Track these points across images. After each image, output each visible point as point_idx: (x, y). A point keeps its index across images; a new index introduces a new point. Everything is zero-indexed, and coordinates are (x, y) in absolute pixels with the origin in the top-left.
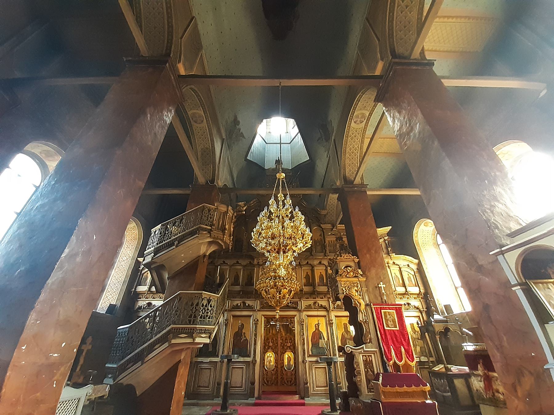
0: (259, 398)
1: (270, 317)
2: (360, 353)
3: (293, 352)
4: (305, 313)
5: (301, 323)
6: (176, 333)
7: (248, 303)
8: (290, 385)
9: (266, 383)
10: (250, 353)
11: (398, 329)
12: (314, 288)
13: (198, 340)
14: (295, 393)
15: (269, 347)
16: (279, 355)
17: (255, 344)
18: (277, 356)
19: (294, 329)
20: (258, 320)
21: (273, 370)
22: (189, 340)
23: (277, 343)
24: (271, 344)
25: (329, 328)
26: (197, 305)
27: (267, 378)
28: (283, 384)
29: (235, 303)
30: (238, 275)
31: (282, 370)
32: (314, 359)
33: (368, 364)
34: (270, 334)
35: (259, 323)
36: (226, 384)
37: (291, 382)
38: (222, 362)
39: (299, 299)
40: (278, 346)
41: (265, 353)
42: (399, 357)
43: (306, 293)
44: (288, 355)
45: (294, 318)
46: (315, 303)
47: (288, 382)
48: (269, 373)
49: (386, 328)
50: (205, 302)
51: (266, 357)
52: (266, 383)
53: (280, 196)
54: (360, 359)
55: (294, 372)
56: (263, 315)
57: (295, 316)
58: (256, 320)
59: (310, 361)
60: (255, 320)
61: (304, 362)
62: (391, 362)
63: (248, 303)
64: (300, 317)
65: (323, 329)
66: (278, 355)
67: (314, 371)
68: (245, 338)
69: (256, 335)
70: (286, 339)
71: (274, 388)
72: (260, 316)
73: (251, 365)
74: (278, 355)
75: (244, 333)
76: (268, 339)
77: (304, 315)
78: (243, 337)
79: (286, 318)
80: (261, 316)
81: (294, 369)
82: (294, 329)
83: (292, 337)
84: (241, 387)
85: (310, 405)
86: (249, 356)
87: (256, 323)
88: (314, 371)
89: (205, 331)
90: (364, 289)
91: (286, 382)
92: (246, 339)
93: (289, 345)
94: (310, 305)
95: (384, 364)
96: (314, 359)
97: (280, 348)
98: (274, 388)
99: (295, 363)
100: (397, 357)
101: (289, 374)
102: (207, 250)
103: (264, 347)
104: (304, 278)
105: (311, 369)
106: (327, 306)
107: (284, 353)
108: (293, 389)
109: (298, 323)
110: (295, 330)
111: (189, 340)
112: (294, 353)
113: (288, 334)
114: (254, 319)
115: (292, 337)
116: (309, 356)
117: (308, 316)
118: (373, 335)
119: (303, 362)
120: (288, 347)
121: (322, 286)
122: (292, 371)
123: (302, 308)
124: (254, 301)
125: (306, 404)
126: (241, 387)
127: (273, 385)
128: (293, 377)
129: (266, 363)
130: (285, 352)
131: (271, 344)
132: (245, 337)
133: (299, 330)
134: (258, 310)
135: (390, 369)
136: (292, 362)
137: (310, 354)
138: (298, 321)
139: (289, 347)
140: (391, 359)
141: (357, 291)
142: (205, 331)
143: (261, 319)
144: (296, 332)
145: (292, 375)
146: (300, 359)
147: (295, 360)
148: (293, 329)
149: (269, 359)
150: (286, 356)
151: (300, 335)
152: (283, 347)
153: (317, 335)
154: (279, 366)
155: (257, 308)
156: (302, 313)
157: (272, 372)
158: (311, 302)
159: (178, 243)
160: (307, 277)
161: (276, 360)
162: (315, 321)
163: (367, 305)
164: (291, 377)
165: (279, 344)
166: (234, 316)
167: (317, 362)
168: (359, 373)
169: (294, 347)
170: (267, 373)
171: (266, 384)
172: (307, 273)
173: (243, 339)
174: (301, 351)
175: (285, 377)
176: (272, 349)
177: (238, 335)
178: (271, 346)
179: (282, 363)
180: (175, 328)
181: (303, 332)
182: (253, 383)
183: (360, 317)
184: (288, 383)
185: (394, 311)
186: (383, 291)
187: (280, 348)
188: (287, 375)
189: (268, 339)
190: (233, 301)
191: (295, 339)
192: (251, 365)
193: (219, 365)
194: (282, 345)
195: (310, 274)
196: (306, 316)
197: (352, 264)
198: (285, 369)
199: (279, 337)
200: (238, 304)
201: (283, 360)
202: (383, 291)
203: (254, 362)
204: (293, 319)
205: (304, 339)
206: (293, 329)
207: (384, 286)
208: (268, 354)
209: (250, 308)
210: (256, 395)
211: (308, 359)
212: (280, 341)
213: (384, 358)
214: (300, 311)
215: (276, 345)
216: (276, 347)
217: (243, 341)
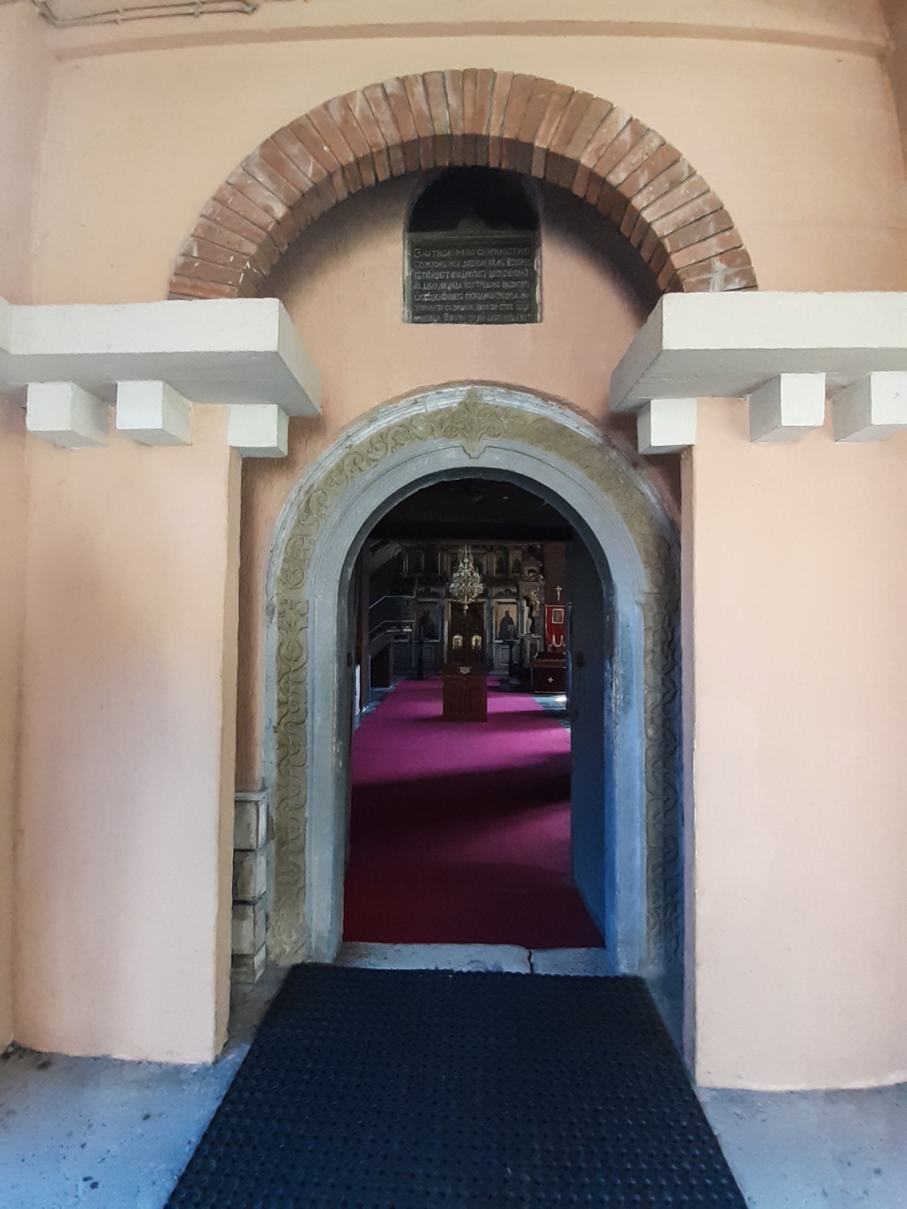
2: (529, 639)
4: (495, 600)
5: (490, 610)
6: (389, 626)
7: (432, 589)
10: (438, 634)
11: (562, 623)
13: (405, 630)
22: (399, 631)
26: (400, 606)
32: (501, 641)
33: (533, 646)
35: (446, 608)
36: (421, 660)
38: (410, 642)
42: (558, 642)
43: (497, 580)
46: (506, 591)
49: (553, 622)
50: (405, 604)
51: (454, 640)
53: (466, 560)
54: (528, 643)
56: (451, 602)
57: (485, 602)
61: (491, 643)
62: (551, 645)
63: (432, 589)
65: (513, 616)
72: (447, 604)
86: (437, 638)
87: (442, 609)
89: (408, 624)
90: (542, 592)
93: (477, 629)
95: (546, 647)
96: (501, 641)
100: (556, 641)
102: (395, 553)
104: (496, 563)
111: (399, 631)
116: (497, 639)
117: (499, 603)
118: (541, 627)
130: (474, 635)
135: (549, 650)
137: (498, 637)
138: (487, 608)
140: (551, 644)
141: (535, 593)
142: (408, 624)
144: (485, 618)
146: (488, 641)
147: (482, 640)
150: (474, 639)
153: (507, 620)
158: (502, 590)
159: (373, 554)
160: (499, 563)
161: (463, 641)
162: (504, 608)
163: (541, 604)
168: (526, 652)
169: (482, 632)
172: (501, 558)
177: (424, 621)
180: (388, 623)
183: (534, 614)
185: (563, 610)
186: (559, 593)
191: (483, 625)
195: (503, 557)
197: (536, 568)
200: (421, 592)
201: (471, 642)
202: (559, 593)
205: (492, 624)
207: (561, 589)
209: (436, 595)
211: (494, 641)
213: (546, 641)
214: (489, 598)
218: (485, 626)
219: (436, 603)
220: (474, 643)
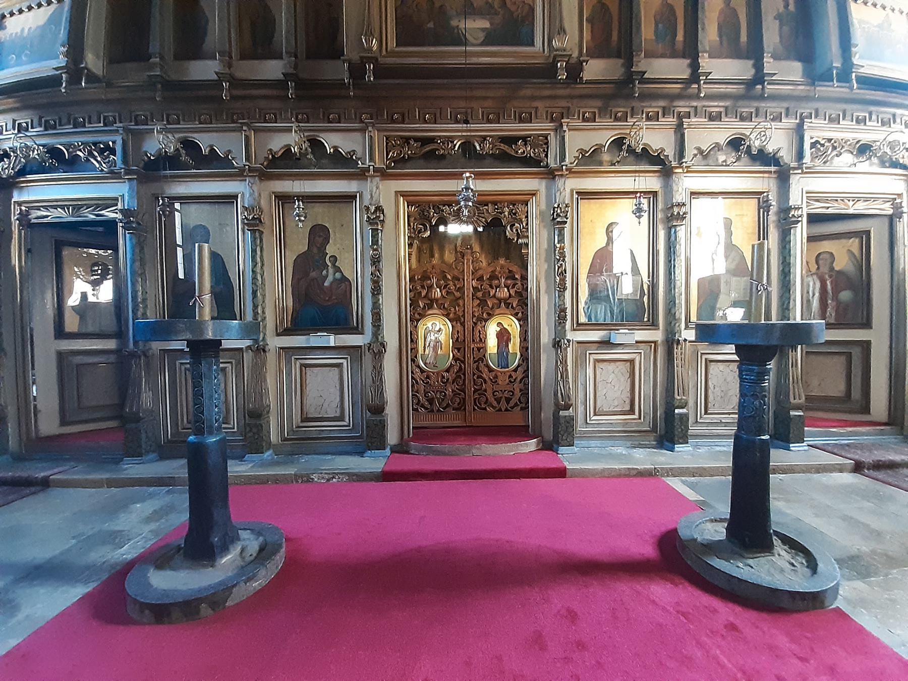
0: (401, 449)
1: (429, 203)
3: (520, 315)
4: (572, 184)
8: (506, 410)
9: (423, 406)
10: (361, 320)
12: (629, 63)
14: (520, 433)
15: (432, 301)
16: (469, 324)
17: (377, 290)
18: (459, 327)
19: (525, 240)
20: (379, 209)
21: (448, 371)
23: (461, 289)
24: (437, 293)
25: (662, 234)
27: (426, 393)
28: (483, 406)
29: (277, 143)
30: (267, 8)
31: (478, 368)
32: (595, 336)
34: (435, 261)
37: (508, 400)
39: (552, 121)
40: (462, 297)
41: (418, 321)
44: (499, 324)
45: (526, 203)
47: (498, 401)
48: (433, 377)
52: (423, 406)
55: (519, 375)
56: (404, 194)
57: (533, 194)
58: (373, 209)
59: (578, 342)
60: (368, 209)
64: (550, 197)
66: (463, 324)
67: (590, 371)
68: (338, 275)
69: (376, 261)
70: (493, 277)
71: (452, 420)
73: (368, 359)
74: (463, 324)
75: (334, 259)
76: (425, 277)
77: (568, 191)
78: (331, 270)
79: (495, 203)
80: (393, 194)
81: (519, 366)
82: (525, 240)
83: (515, 268)
84: (341, 418)
85: (583, 474)
86: (357, 330)
87: (376, 216)
88: (590, 371)
91: (492, 399)
92: (344, 279)
93: (503, 293)
94: (598, 150)
96: (595, 336)
97: (470, 305)
98: (452, 420)
99: (524, 349)
101: (503, 381)
103: (414, 303)
105: (580, 361)
106: (670, 152)
107: (486, 320)
108: (515, 418)
109: (542, 221)
110: (527, 245)
112: (523, 320)
113: (502, 261)
114: (366, 203)
115: (515, 268)
116: (579, 326)
119: (557, 344)
120: (500, 300)
121: (663, 56)
122: (515, 370)
123: (563, 159)
124: (357, 136)
125: (568, 473)
126: (341, 418)
127: (450, 410)
128: (517, 386)
129: (421, 351)
130: (490, 315)
131: (437, 293)
132: (338, 270)
133: (545, 245)
134: (376, 170)
136: (514, 346)
139: (505, 300)
143: (393, 210)
145: (510, 381)
146: (546, 337)
148: (520, 241)
149: (432, 337)
150: (492, 330)
151: (547, 260)
152: (483, 303)
154: (469, 360)
155: (372, 159)
156: (560, 182)
157: (445, 374)
164: (509, 388)
165: (468, 292)
166: (284, 199)
167: (606, 344)
169: (523, 303)
170: (428, 377)
171: (426, 409)
173: (330, 278)
174: (548, 314)
175: (488, 386)
176: (441, 307)
178: (437, 300)
179: (479, 349)
181: (562, 248)
182: (378, 409)
184: (499, 403)
187: (470, 305)
188: (495, 381)
189: (425, 277)
190: (262, 135)
191: (524, 278)
192: (368, 359)
193: (248, 357)
194: (480, 294)
196: (575, 196)
198: (488, 366)
199: (468, 268)
201: (483, 340)
203: (377, 349)
204: (521, 207)
205: (563, 274)
206: (520, 241)
208: (429, 325)
210: (392, 437)
211: (570, 335)
212: (470, 283)
214: (551, 175)
215: (458, 294)
216: (455, 301)
217: (332, 283)
218: (532, 284)
219: (349, 198)
220: (492, 343)
